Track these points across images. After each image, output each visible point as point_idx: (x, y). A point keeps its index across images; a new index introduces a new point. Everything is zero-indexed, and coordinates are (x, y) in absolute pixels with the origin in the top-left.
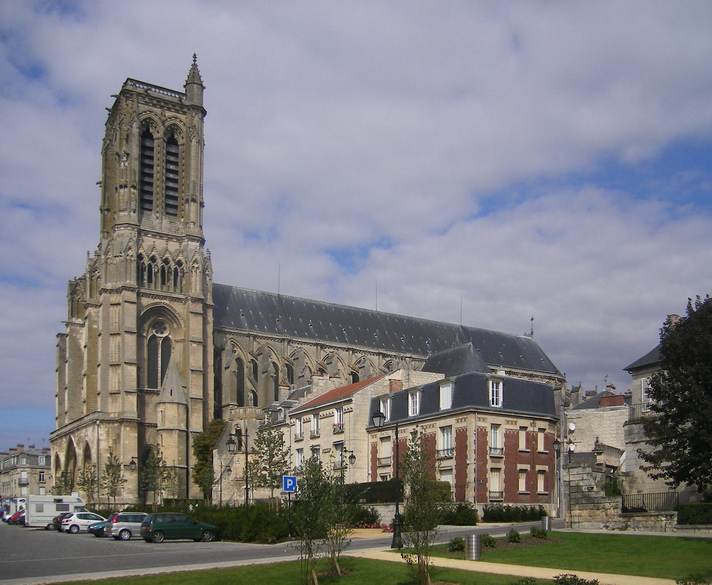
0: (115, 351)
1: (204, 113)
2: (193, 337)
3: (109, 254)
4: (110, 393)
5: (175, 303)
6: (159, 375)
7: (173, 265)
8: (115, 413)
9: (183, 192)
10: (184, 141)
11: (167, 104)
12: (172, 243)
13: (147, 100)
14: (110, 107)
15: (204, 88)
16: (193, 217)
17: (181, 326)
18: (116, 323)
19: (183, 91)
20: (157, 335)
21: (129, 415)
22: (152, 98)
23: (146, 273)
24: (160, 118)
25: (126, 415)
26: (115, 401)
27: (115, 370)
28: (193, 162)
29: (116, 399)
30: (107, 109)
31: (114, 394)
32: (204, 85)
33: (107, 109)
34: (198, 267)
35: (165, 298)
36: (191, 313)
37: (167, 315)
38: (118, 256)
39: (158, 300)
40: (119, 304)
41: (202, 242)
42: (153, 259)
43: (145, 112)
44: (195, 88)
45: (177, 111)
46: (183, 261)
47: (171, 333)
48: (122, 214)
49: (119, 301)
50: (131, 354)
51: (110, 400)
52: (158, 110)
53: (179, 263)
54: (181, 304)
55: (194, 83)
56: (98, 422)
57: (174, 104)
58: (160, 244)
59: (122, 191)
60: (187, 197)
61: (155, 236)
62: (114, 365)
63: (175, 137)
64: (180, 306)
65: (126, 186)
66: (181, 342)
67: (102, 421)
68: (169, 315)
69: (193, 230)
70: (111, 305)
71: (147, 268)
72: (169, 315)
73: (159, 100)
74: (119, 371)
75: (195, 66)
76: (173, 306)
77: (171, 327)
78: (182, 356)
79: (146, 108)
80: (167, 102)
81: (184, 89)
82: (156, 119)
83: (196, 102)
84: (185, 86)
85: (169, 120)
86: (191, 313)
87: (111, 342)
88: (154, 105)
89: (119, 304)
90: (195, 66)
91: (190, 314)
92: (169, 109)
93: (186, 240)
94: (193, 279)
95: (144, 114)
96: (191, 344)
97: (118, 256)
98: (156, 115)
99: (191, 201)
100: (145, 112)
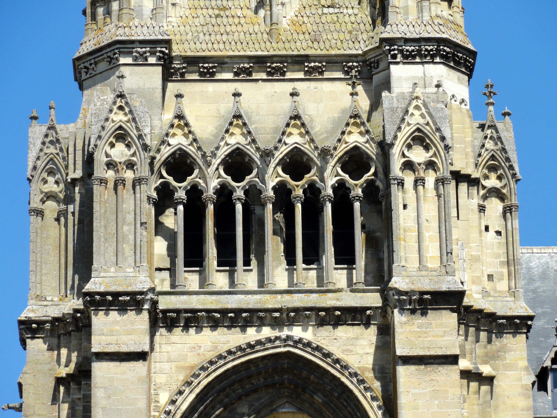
39: (267, 332)
71: (211, 208)
76: (328, 346)
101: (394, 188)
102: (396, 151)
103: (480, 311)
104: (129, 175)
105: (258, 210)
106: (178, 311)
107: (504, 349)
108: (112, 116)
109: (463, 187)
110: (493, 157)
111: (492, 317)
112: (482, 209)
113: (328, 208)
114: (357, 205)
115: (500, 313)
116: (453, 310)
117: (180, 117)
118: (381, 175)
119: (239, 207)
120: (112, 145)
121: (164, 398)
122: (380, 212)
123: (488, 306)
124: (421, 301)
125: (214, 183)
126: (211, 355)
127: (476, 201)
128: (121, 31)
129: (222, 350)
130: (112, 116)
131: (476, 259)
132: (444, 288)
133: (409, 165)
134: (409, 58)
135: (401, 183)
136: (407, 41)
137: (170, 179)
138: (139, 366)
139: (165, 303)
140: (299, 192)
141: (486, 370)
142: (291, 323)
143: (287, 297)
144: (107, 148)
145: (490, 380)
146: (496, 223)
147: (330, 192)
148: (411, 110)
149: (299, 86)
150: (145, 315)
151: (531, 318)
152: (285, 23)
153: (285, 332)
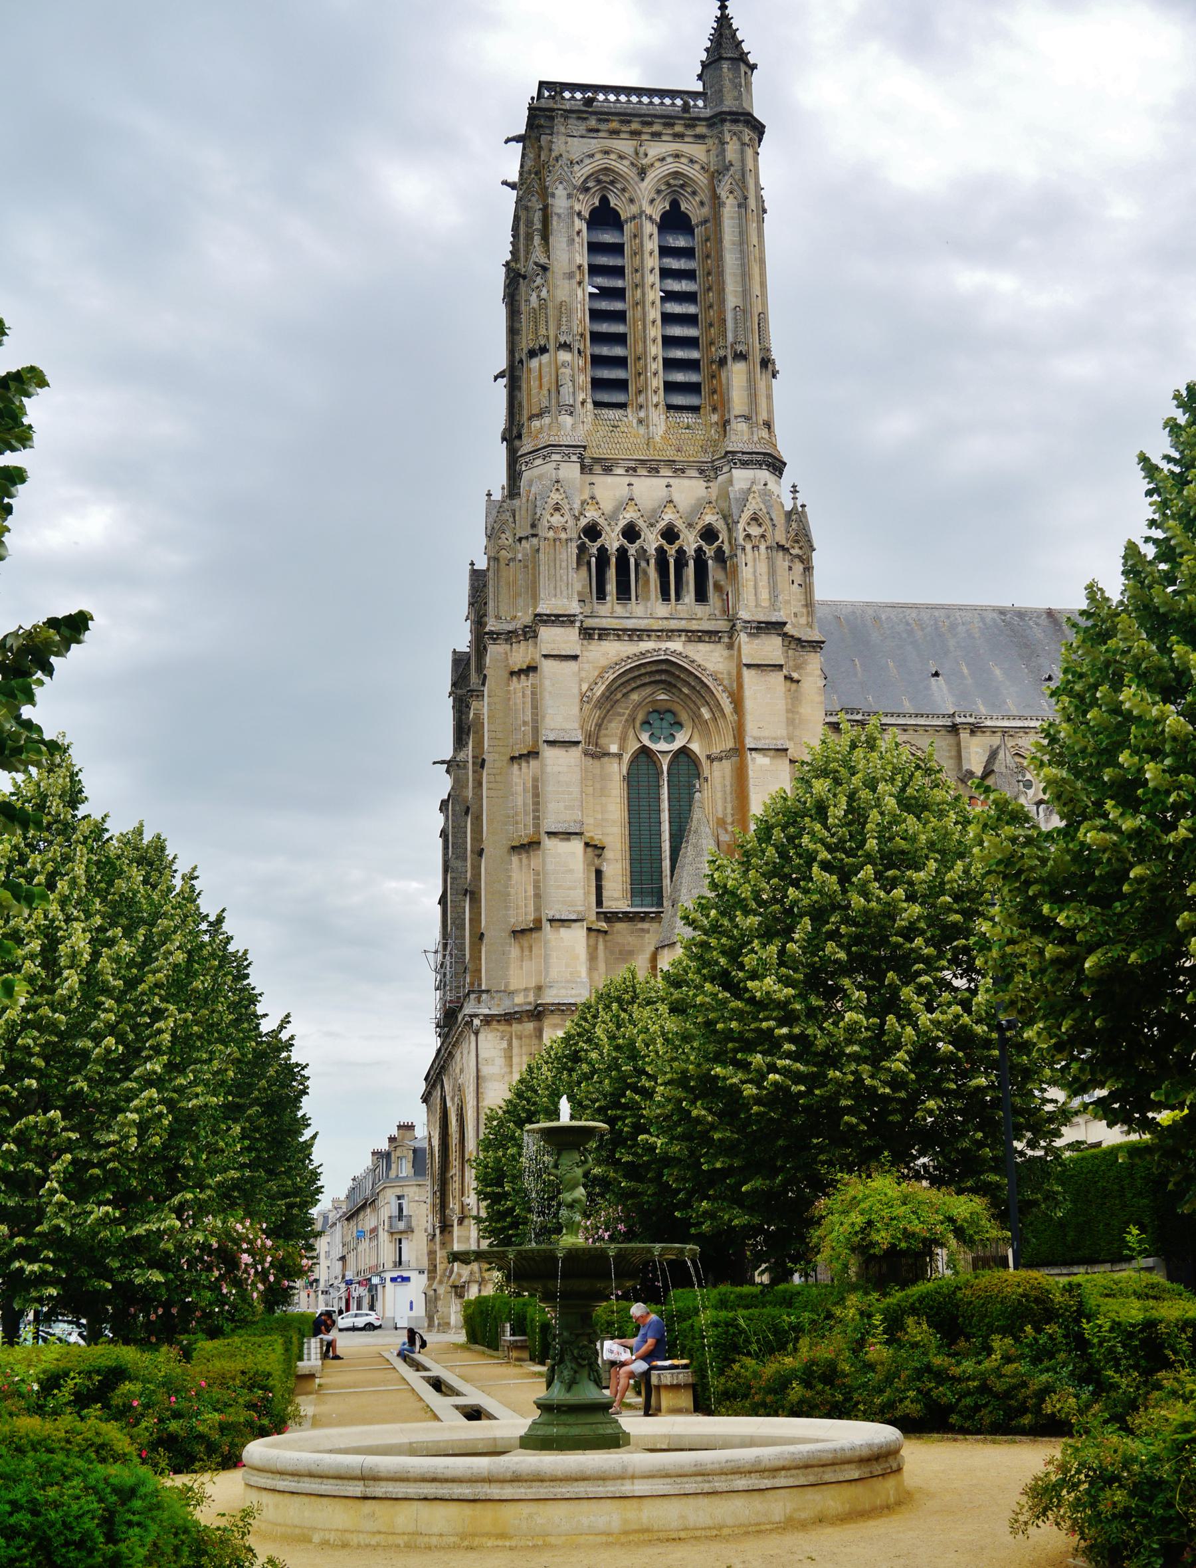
0: (525, 804)
1: (759, 129)
2: (756, 738)
3: (503, 536)
4: (513, 932)
5: (702, 647)
6: (666, 864)
7: (690, 541)
8: (526, 989)
9: (712, 343)
10: (705, 211)
11: (650, 124)
12: (686, 482)
13: (593, 123)
14: (514, 177)
15: (753, 67)
16: (738, 402)
17: (722, 710)
18: (525, 723)
19: (698, 87)
20: (654, 747)
21: (563, 992)
22: (604, 116)
23: (612, 573)
24: (632, 164)
25: (553, 992)
26: (526, 953)
27: (525, 860)
28: (730, 259)
29: (531, 948)
30: (505, 183)
31: (523, 931)
32: (752, 59)
33: (505, 183)
34: (763, 536)
35: (670, 634)
36: (749, 666)
37: (679, 685)
38: (527, 538)
40: (531, 669)
41: (776, 466)
42: (631, 533)
43: (592, 156)
44: (725, 70)
45: (678, 136)
46: (720, 525)
47: (696, 736)
48: (536, 424)
49: (533, 659)
50: (566, 808)
51: (514, 952)
52: (625, 146)
53: (709, 534)
54: (719, 647)
55: (721, 58)
56: (476, 1022)
57: (669, 120)
58: (649, 490)
59: (534, 363)
60: (722, 353)
61: (635, 470)
62: (523, 846)
63: (683, 208)
64: (717, 654)
65: (544, 350)
66: (727, 758)
67: (488, 1020)
68: (688, 684)
69: (741, 437)
70: (512, 673)
71: (613, 560)
72: (688, 684)
73: (625, 117)
74: (535, 861)
75: (723, 22)
77: (696, 717)
78: (729, 799)
79: (594, 144)
80: (647, 119)
81: (700, 83)
82: (623, 167)
83: (729, 104)
84: (700, 77)
85: (657, 164)
86: (749, 666)
87: (515, 779)
88: (614, 133)
89: (531, 669)
90: (723, 22)
91: (745, 671)
92: (656, 135)
93: (725, 469)
94: (746, 573)
95: (587, 161)
96: (753, 759)
97: (527, 538)
98: (621, 157)
99: (734, 359)
100: (592, 156)
101: (739, 552)
102: (740, 526)
103: (792, 636)
104: (563, 536)
105: (643, 564)
106: (594, 629)
107: (805, 662)
108: (552, 495)
109: (781, 554)
110: (796, 535)
111: (799, 640)
112: (790, 568)
113: (691, 563)
114: (710, 562)
115: (804, 638)
116: (779, 635)
117: (593, 498)
118: (726, 543)
119: (632, 560)
120: (552, 515)
121: (585, 687)
122: (725, 568)
123: (797, 634)
124: (758, 628)
125: (616, 545)
126: (615, 659)
127: (787, 564)
128: (552, 438)
129: (624, 655)
130: (552, 495)
131: (788, 602)
132: (774, 620)
133: (748, 536)
134: (745, 464)
135: (744, 549)
136: (743, 453)
137: (586, 540)
138: (572, 665)
139: (590, 623)
140: (673, 552)
141: (795, 675)
142: (669, 638)
143: (665, 622)
144: (548, 517)
145: (798, 681)
146: (798, 580)
147: (693, 553)
148: (750, 498)
149: (672, 481)
150: (577, 631)
151: (823, 642)
152: (658, 439)
153: (664, 645)
